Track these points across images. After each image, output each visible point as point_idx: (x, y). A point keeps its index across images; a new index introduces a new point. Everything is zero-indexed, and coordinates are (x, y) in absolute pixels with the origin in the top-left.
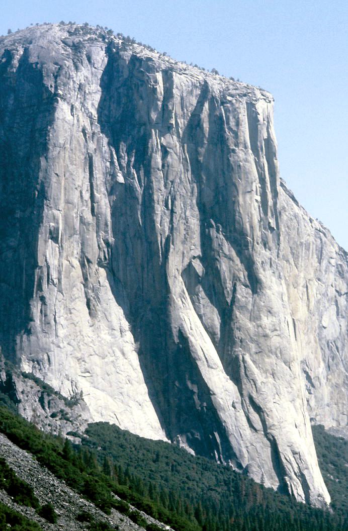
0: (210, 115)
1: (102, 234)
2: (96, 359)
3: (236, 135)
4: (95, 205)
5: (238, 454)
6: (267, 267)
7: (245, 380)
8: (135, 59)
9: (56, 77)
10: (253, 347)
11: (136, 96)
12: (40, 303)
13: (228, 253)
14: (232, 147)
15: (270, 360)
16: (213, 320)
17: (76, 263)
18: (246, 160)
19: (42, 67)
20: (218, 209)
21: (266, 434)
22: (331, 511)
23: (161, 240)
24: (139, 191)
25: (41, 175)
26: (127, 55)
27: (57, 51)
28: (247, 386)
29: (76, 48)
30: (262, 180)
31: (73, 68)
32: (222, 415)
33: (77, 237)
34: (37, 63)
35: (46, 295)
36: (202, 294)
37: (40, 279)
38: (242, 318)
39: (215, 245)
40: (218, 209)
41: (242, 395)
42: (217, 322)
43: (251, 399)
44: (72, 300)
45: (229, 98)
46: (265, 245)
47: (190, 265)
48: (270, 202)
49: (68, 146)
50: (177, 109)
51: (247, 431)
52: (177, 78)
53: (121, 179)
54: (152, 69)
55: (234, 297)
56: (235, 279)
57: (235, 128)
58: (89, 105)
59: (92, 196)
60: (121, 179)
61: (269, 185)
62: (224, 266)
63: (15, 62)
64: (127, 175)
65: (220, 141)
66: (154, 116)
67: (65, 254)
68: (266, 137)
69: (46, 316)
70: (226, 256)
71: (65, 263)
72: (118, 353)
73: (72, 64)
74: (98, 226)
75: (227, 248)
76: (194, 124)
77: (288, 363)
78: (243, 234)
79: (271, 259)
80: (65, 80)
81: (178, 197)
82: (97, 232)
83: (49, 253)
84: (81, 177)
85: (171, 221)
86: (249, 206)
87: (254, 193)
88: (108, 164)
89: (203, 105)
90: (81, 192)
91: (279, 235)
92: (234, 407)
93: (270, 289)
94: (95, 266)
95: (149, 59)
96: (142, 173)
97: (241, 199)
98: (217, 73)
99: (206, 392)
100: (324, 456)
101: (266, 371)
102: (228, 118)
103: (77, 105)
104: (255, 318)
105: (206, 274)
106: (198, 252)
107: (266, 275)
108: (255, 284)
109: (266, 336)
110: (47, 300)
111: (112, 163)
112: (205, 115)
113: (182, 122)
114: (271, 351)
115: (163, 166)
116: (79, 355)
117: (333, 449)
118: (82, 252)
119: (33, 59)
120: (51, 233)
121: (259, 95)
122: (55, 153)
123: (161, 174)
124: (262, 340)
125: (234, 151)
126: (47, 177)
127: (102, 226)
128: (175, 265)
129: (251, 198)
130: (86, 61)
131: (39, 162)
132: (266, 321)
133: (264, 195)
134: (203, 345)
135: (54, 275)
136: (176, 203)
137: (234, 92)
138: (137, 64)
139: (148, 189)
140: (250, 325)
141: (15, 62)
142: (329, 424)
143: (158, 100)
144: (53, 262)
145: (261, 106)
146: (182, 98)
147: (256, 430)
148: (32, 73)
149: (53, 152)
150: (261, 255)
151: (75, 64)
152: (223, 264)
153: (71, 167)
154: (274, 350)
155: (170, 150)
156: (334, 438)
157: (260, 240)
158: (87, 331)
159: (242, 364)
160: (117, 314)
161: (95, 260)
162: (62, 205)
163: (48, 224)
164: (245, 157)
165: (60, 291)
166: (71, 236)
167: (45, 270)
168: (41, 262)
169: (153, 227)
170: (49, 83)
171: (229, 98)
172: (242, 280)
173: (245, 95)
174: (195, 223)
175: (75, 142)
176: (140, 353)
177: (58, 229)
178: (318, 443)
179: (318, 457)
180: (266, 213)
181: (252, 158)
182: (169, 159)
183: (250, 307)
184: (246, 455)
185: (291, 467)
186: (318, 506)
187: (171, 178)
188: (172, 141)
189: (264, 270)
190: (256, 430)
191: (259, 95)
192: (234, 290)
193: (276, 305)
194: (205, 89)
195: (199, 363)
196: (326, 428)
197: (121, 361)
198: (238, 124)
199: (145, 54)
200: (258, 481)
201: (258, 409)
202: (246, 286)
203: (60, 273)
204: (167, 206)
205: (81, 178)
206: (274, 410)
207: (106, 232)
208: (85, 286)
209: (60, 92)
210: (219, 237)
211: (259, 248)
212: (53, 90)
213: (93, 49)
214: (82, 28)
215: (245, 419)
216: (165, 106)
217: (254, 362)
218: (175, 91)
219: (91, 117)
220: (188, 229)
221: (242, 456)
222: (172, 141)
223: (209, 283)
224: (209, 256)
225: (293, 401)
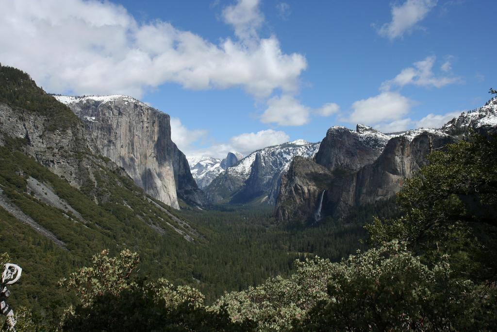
15: (168, 176)
144: (122, 153)
177: (122, 145)
201: (166, 187)
205: (128, 134)
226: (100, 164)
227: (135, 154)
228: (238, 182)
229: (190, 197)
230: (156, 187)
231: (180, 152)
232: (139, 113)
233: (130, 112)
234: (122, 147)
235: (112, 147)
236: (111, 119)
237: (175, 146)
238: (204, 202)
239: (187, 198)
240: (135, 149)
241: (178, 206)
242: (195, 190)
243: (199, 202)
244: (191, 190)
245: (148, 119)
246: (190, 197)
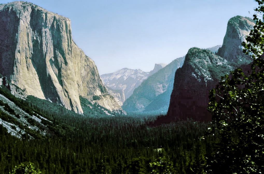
0: (56, 24)
1: (30, 51)
2: (29, 81)
3: (62, 28)
4: (29, 45)
5: (62, 102)
6: (69, 59)
7: (64, 85)
8: (38, 10)
9: (20, 14)
10: (66, 78)
11: (39, 19)
12: (16, 67)
13: (60, 56)
14: (61, 31)
15: (69, 81)
16: (56, 71)
17: (24, 58)
18: (64, 35)
19: (16, 12)
20: (58, 46)
21: (69, 98)
22: (83, 115)
23: (44, 53)
24: (39, 41)
25: (16, 37)
26: (36, 9)
27: (20, 8)
28: (64, 86)
29: (24, 7)
30: (68, 39)
31: (23, 12)
32: (58, 93)
33: (24, 52)
34: (15, 11)
35: (17, 66)
36: (54, 65)
37: (16, 62)
38: (63, 71)
39: (57, 54)
40: (58, 46)
41: (63, 89)
42: (57, 72)
43: (65, 89)
44: (23, 67)
45: (60, 20)
46: (68, 54)
47: (51, 59)
48: (70, 44)
49: (23, 31)
50: (49, 22)
51: (64, 97)
52: (48, 15)
53: (35, 38)
54: (42, 13)
55: (61, 66)
56: (62, 62)
57: (62, 27)
58: (27, 21)
59: (28, 42)
60: (35, 38)
61: (69, 40)
62: (59, 59)
63: (10, 10)
64: (37, 38)
65: (58, 30)
66: (43, 24)
67: (22, 56)
68: (69, 29)
69: (17, 70)
70: (59, 57)
71: (22, 58)
72: (34, 79)
73: (23, 11)
74: (29, 49)
75: (60, 55)
76: (53, 26)
77: (74, 81)
78: (64, 52)
79: (70, 58)
80: (22, 15)
81: (48, 43)
82: (29, 51)
83: (18, 55)
84: (26, 38)
85: (47, 49)
86: (65, 45)
87: (66, 42)
88: (32, 35)
89: (54, 22)
90: (26, 42)
91: (72, 52)
92: (61, 91)
93: (70, 64)
94: (29, 59)
95: (41, 10)
96: (40, 37)
98: (57, 14)
99: (55, 88)
100: (82, 103)
101: (69, 83)
102: (60, 25)
103: (25, 21)
104: (66, 71)
105: (55, 61)
106: (53, 56)
107: (68, 61)
108: (66, 63)
109: (68, 75)
110: (18, 67)
111: (33, 35)
112: (55, 24)
113: (50, 26)
114: (70, 79)
115: (45, 36)
116: (25, 80)
117: (84, 101)
118: (26, 56)
119: (14, 10)
120: (18, 51)
121: (67, 20)
122: (20, 32)
123: (44, 37)
124: (68, 76)
125: (62, 32)
126: (17, 38)
127: (31, 50)
129: (65, 43)
130: (26, 10)
131: (16, 34)
132: (69, 72)
133: (68, 43)
134: (54, 78)
135: (19, 61)
136: (48, 44)
137: (61, 19)
138: (39, 12)
139: (41, 41)
140: (65, 73)
141: (10, 10)
142: (83, 95)
143: (44, 20)
144: (19, 58)
145: (68, 22)
146: (49, 20)
147: (66, 97)
148: (14, 13)
149: (19, 32)
150: (67, 57)
151: (24, 11)
152: (59, 59)
153: (23, 36)
154: (70, 78)
155: (47, 33)
156: (84, 98)
157: (67, 53)
158: (27, 74)
159: (63, 82)
160: (34, 70)
161: (29, 57)
162: (21, 44)
163: (18, 49)
164: (64, 34)
165: (21, 65)
166: (23, 52)
167: (17, 59)
168: (16, 58)
169: (42, 50)
170: (18, 15)
171: (60, 20)
172: (63, 62)
173: (64, 19)
174: (52, 49)
175: (24, 30)
176: (39, 79)
177: (20, 50)
178: (80, 100)
179: (80, 103)
180: (69, 47)
181: (66, 34)
182: (46, 34)
183: (65, 68)
184: (64, 102)
185: (74, 105)
186: (80, 114)
187: (47, 38)
188: (47, 30)
189: (68, 60)
190: (66, 97)
191: (67, 20)
192: (61, 65)
193: (71, 68)
194: (55, 17)
195: (53, 81)
196: (82, 96)
197: (35, 81)
198: (63, 26)
199: (40, 9)
200: (67, 108)
202: (64, 64)
203: (20, 60)
204: (46, 45)
206: (70, 92)
207: (31, 51)
208: (27, 63)
209: (21, 18)
210: (58, 52)
211: (67, 55)
212: (19, 17)
213: (28, 7)
214: (26, 3)
215: (64, 94)
216: (45, 22)
217: (66, 81)
218: (48, 18)
219: (28, 24)
220: (50, 50)
221: (63, 103)
222: (47, 30)
223: (55, 63)
224: (55, 57)
225: (75, 90)
228: (158, 90)
230: (56, 92)
231: (86, 57)
237: (81, 51)
238: (113, 107)
242: (104, 96)
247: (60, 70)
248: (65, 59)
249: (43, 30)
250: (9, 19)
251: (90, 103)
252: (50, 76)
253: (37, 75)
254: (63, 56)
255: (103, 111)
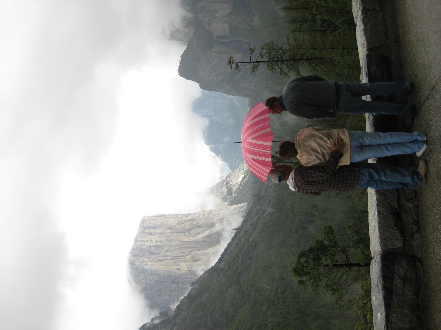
10: (207, 221)
17: (186, 264)
30: (165, 218)
48: (171, 216)
52: (139, 239)
62: (187, 228)
76: (151, 234)
97: (170, 223)
103: (145, 263)
106: (183, 234)
128: (187, 239)
132: (201, 217)
134: (207, 233)
135: (189, 269)
140: (202, 221)
144: (186, 269)
168: (185, 272)
174: (176, 235)
203: (188, 268)
211: (182, 219)
226: (181, 321)
227: (187, 254)
229: (235, 188)
232: (141, 251)
233: (141, 260)
234: (178, 269)
235: (180, 280)
236: (149, 281)
239: (236, 192)
240: (180, 255)
241: (243, 204)
242: (227, 183)
243: (240, 179)
244: (227, 188)
245: (147, 241)
246: (235, 188)
247: (200, 227)
248: (186, 221)
249: (154, 243)
250: (143, 281)
251: (236, 198)
252: (205, 237)
253: (205, 251)
254: (183, 223)
255: (244, 183)
